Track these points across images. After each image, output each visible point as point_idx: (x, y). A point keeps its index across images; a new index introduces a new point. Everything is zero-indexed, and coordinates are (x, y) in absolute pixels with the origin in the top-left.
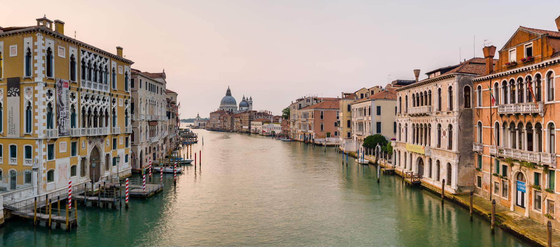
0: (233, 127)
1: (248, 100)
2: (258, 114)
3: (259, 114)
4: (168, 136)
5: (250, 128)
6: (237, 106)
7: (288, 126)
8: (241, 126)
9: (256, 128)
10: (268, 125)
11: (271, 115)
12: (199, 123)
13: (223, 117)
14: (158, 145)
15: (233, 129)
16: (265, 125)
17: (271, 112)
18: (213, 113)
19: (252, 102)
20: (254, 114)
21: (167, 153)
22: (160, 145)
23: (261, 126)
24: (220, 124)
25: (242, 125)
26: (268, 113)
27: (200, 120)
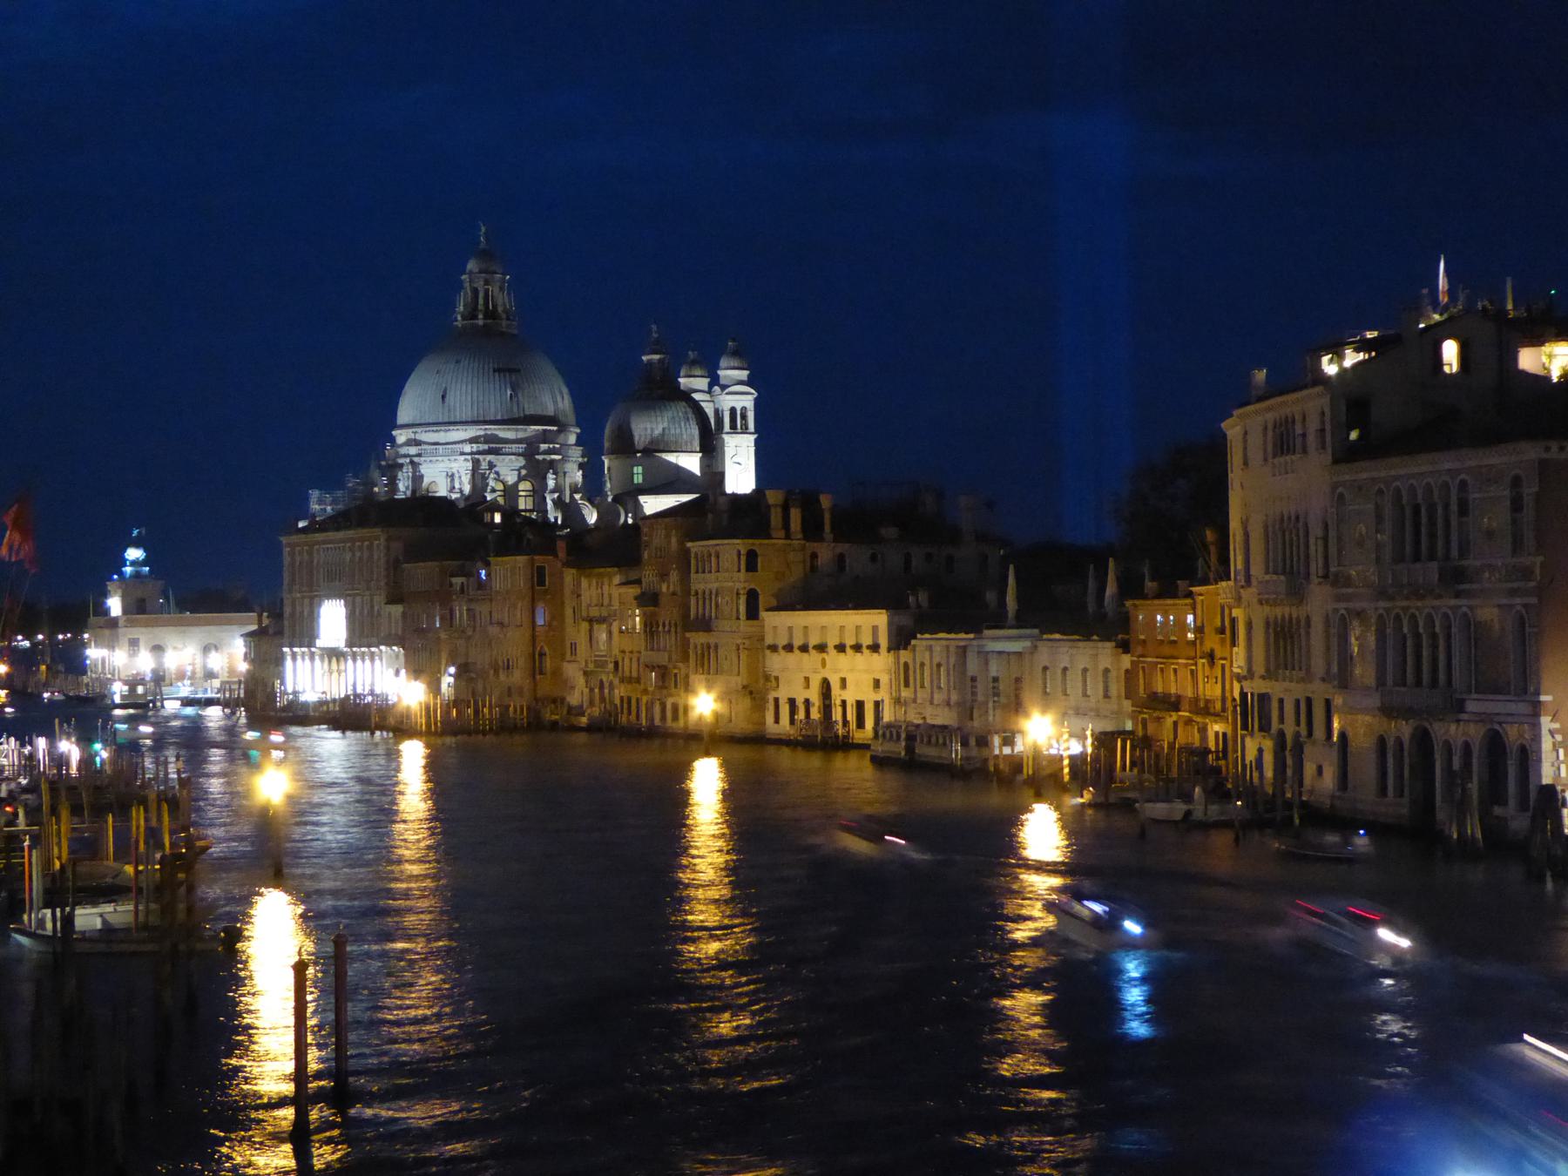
0: (557, 673)
7: (1211, 657)
9: (826, 687)
15: (558, 701)
23: (881, 664)
25: (662, 658)
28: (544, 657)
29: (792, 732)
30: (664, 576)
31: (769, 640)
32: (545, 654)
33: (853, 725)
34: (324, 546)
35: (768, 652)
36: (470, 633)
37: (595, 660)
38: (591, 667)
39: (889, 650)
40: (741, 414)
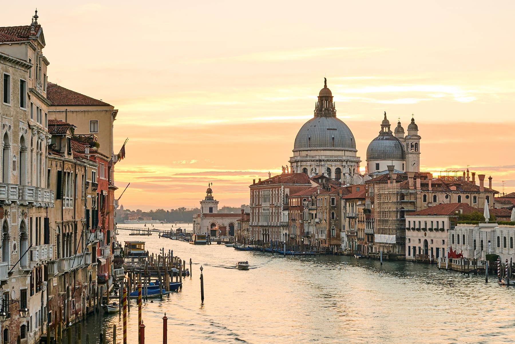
0: (338, 236)
1: (403, 132)
2: (433, 185)
3: (439, 185)
4: (53, 263)
5: (401, 241)
6: (358, 155)
8: (368, 234)
9: (426, 241)
10: (472, 231)
11: (490, 191)
12: (213, 225)
13: (301, 198)
14: (7, 294)
15: (339, 246)
16: (462, 228)
17: (490, 179)
18: (261, 183)
19: (420, 138)
20: (418, 185)
21: (49, 329)
22: (15, 295)
23: (445, 235)
24: (286, 226)
25: (371, 231)
26: (478, 183)
27: (215, 212)
28: (333, 230)
29: (414, 259)
30: (373, 203)
31: (407, 226)
32: (334, 229)
33: (435, 257)
34: (264, 190)
35: (407, 231)
36: (309, 221)
37: (351, 232)
38: (349, 234)
39: (447, 230)
40: (415, 146)
